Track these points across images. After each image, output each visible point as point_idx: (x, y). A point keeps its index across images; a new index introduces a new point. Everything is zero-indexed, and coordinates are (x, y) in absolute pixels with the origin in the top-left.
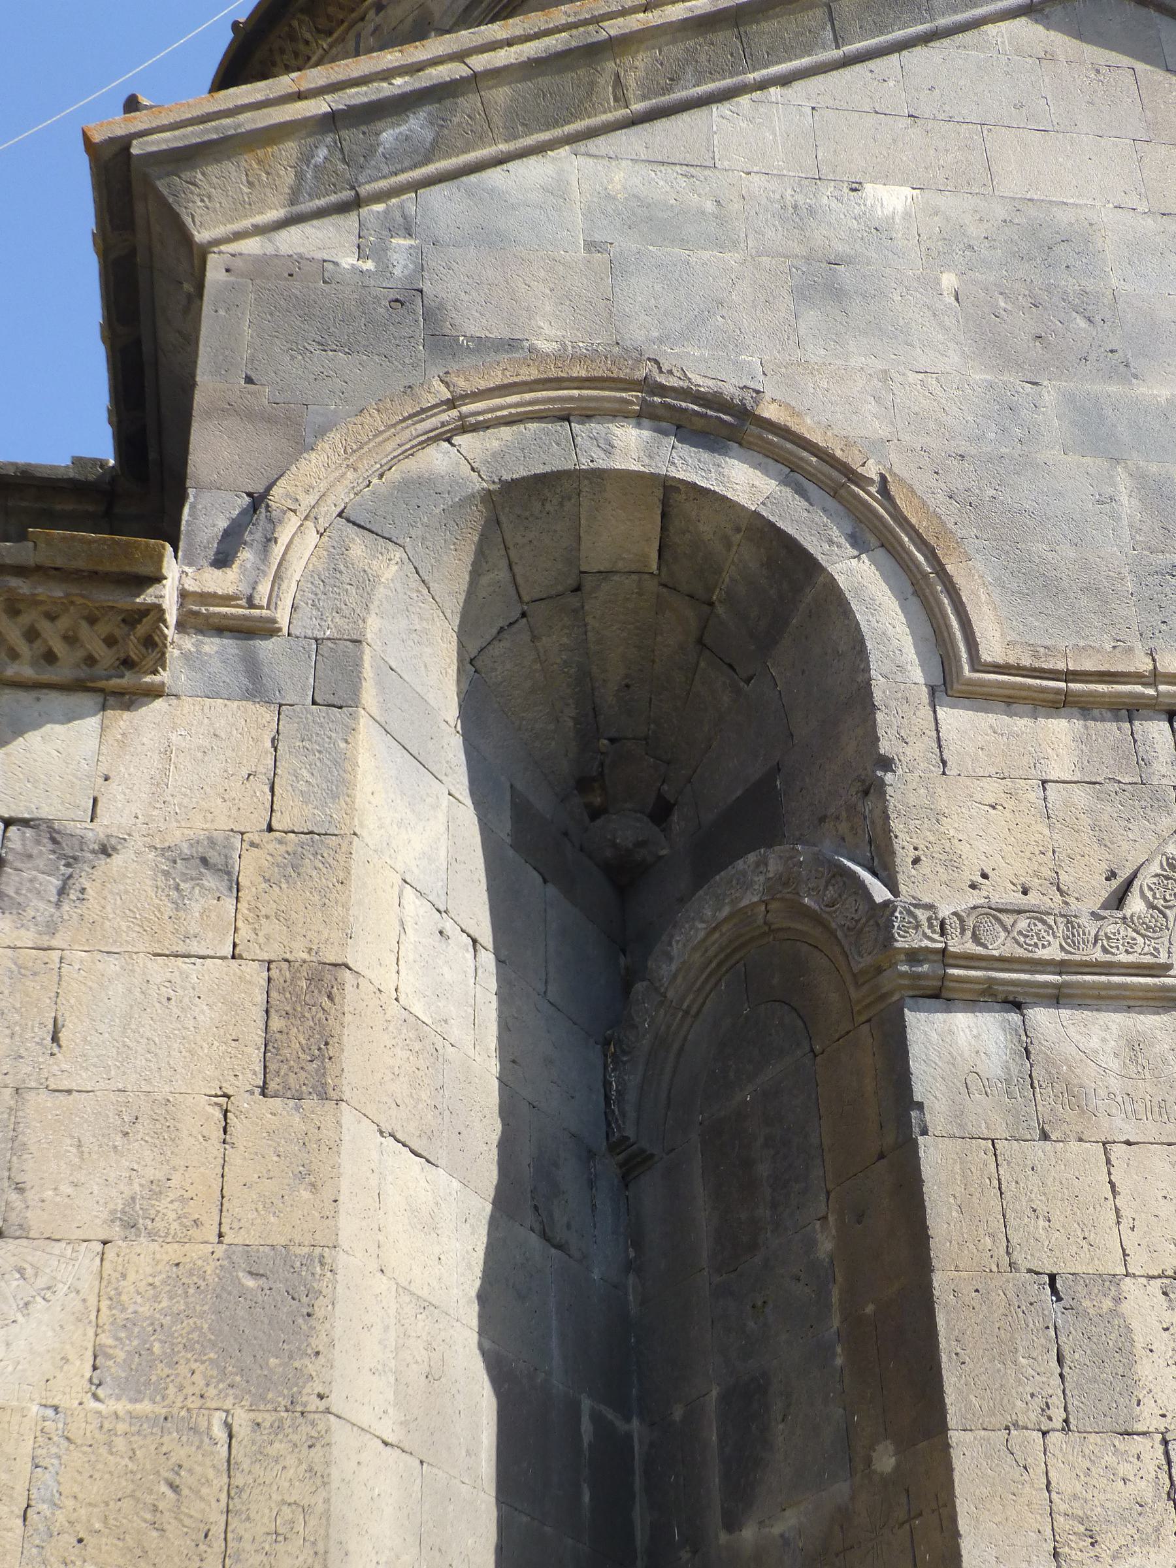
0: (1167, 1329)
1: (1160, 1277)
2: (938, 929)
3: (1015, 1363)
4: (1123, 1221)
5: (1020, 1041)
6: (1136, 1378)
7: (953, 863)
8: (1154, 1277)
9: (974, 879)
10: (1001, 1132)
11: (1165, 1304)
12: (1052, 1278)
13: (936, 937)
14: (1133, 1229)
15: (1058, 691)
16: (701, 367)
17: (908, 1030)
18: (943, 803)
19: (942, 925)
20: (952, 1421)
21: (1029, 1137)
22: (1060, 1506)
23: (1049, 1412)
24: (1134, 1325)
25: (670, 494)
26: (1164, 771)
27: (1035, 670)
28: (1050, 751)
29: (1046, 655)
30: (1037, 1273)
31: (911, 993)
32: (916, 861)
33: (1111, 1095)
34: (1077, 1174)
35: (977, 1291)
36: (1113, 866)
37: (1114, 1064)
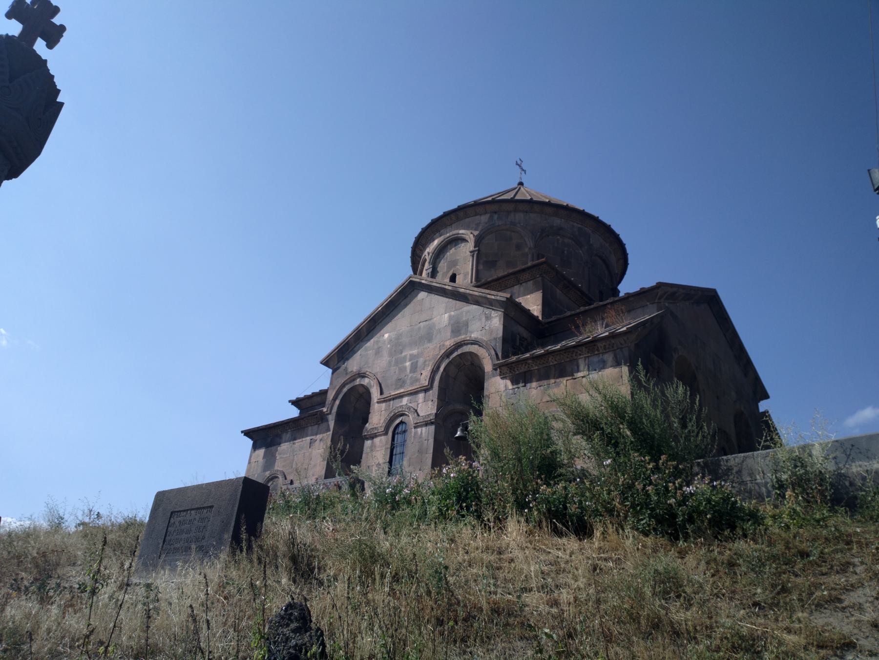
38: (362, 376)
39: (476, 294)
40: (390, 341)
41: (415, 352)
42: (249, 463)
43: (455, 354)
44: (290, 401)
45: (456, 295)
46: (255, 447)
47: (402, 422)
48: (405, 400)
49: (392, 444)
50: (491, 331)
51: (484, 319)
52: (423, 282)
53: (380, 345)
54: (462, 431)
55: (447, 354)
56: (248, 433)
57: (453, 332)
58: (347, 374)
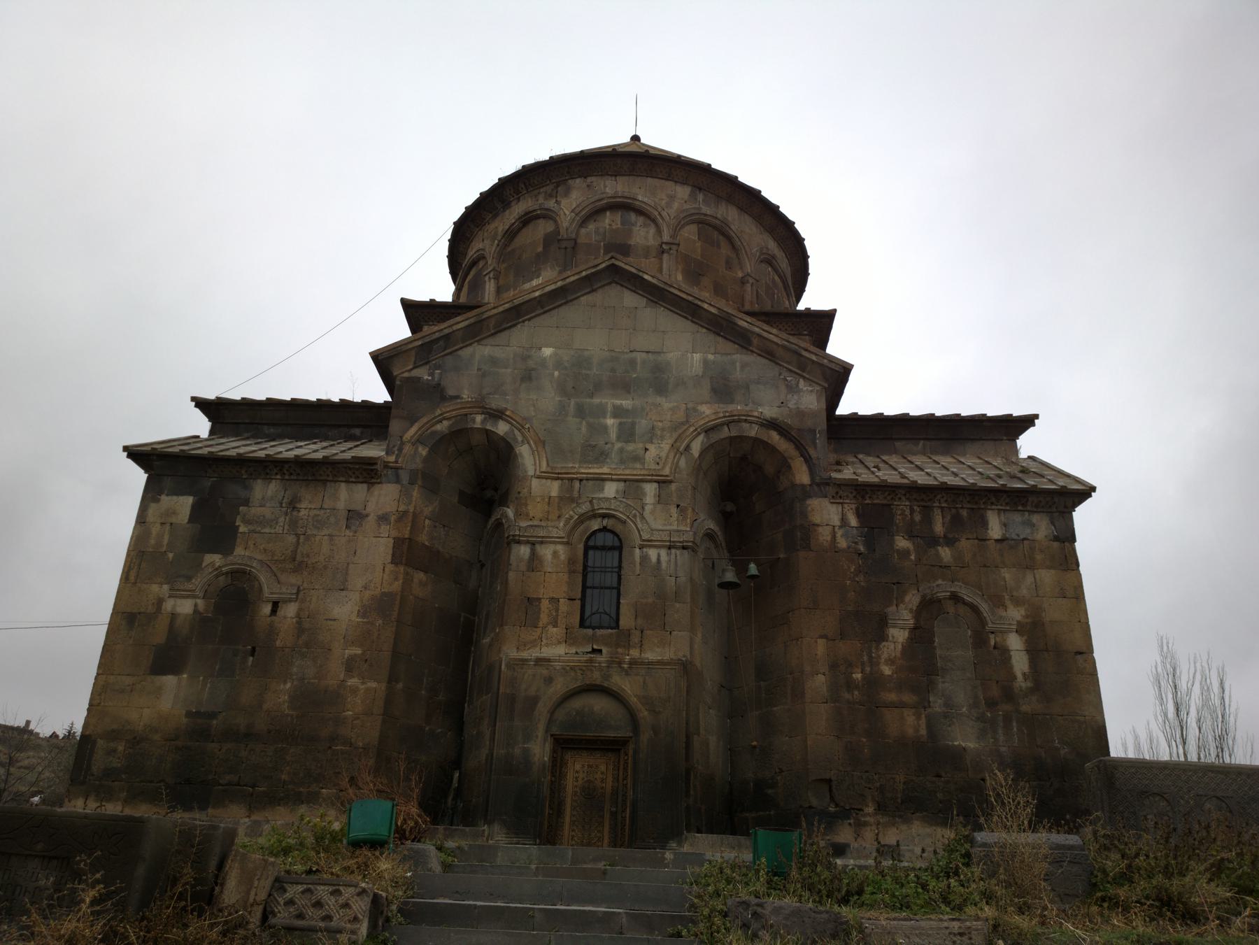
7: (527, 515)
16: (495, 403)
25: (487, 431)
38: (497, 415)
39: (771, 337)
40: (559, 365)
41: (626, 403)
42: (141, 519)
43: (725, 433)
44: (193, 399)
45: (721, 327)
46: (151, 493)
47: (604, 529)
48: (611, 490)
49: (585, 567)
50: (801, 414)
51: (783, 388)
52: (646, 277)
53: (531, 363)
54: (738, 574)
55: (708, 431)
56: (137, 454)
57: (714, 390)
58: (444, 398)
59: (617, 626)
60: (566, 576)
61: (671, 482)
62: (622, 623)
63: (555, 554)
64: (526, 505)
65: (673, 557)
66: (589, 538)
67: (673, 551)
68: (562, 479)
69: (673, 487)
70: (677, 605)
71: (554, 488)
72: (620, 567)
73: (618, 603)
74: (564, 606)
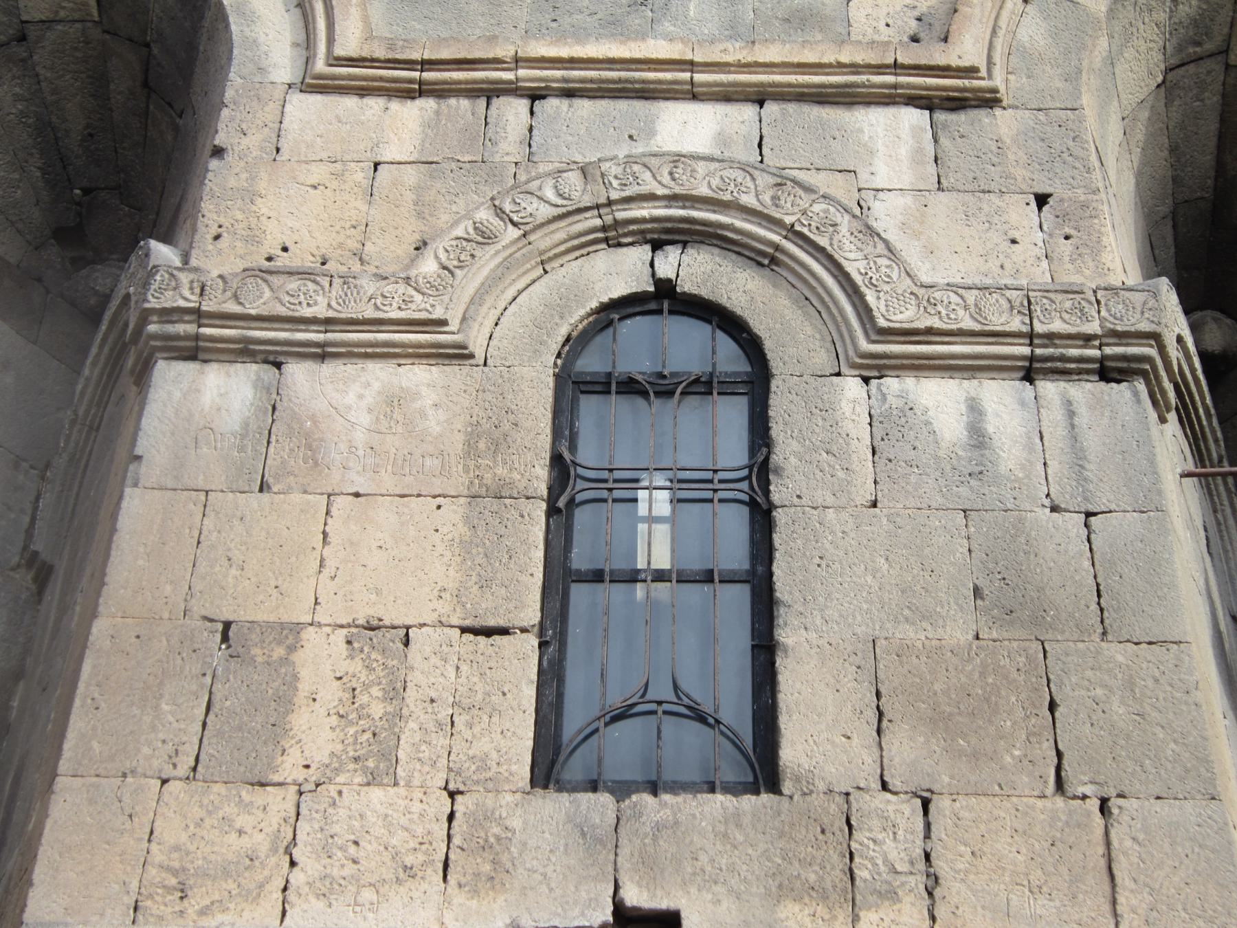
0: (340, 678)
1: (349, 626)
2: (197, 291)
3: (157, 708)
4: (327, 572)
5: (269, 400)
6: (287, 727)
7: (253, 238)
8: (342, 626)
9: (272, 251)
10: (218, 482)
11: (345, 653)
12: (227, 625)
13: (193, 298)
14: (333, 578)
15: (411, 81)
17: (152, 390)
18: (262, 186)
19: (202, 290)
20: (63, 766)
21: (246, 489)
22: (158, 855)
23: (174, 760)
24: (304, 673)
26: (509, 149)
27: (388, 61)
28: (392, 135)
29: (403, 47)
30: (211, 620)
31: (166, 355)
32: (217, 237)
33: (352, 448)
34: (289, 524)
35: (138, 637)
36: (425, 237)
37: (365, 419)
59: (764, 772)
60: (453, 513)
61: (989, 101)
62: (792, 752)
63: (394, 401)
64: (252, 196)
65: (1054, 416)
66: (575, 344)
67: (1049, 388)
68: (440, 92)
69: (1003, 122)
70: (1117, 653)
71: (404, 125)
72: (761, 468)
73: (765, 651)
74: (436, 666)
